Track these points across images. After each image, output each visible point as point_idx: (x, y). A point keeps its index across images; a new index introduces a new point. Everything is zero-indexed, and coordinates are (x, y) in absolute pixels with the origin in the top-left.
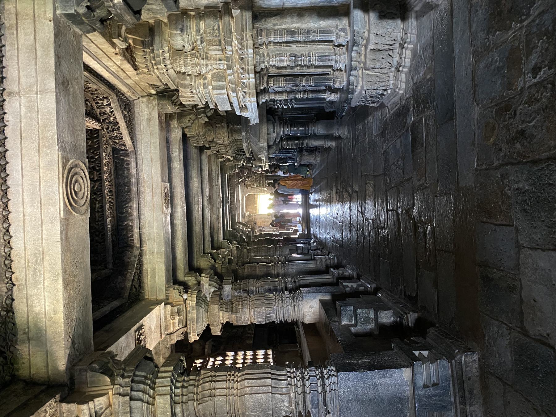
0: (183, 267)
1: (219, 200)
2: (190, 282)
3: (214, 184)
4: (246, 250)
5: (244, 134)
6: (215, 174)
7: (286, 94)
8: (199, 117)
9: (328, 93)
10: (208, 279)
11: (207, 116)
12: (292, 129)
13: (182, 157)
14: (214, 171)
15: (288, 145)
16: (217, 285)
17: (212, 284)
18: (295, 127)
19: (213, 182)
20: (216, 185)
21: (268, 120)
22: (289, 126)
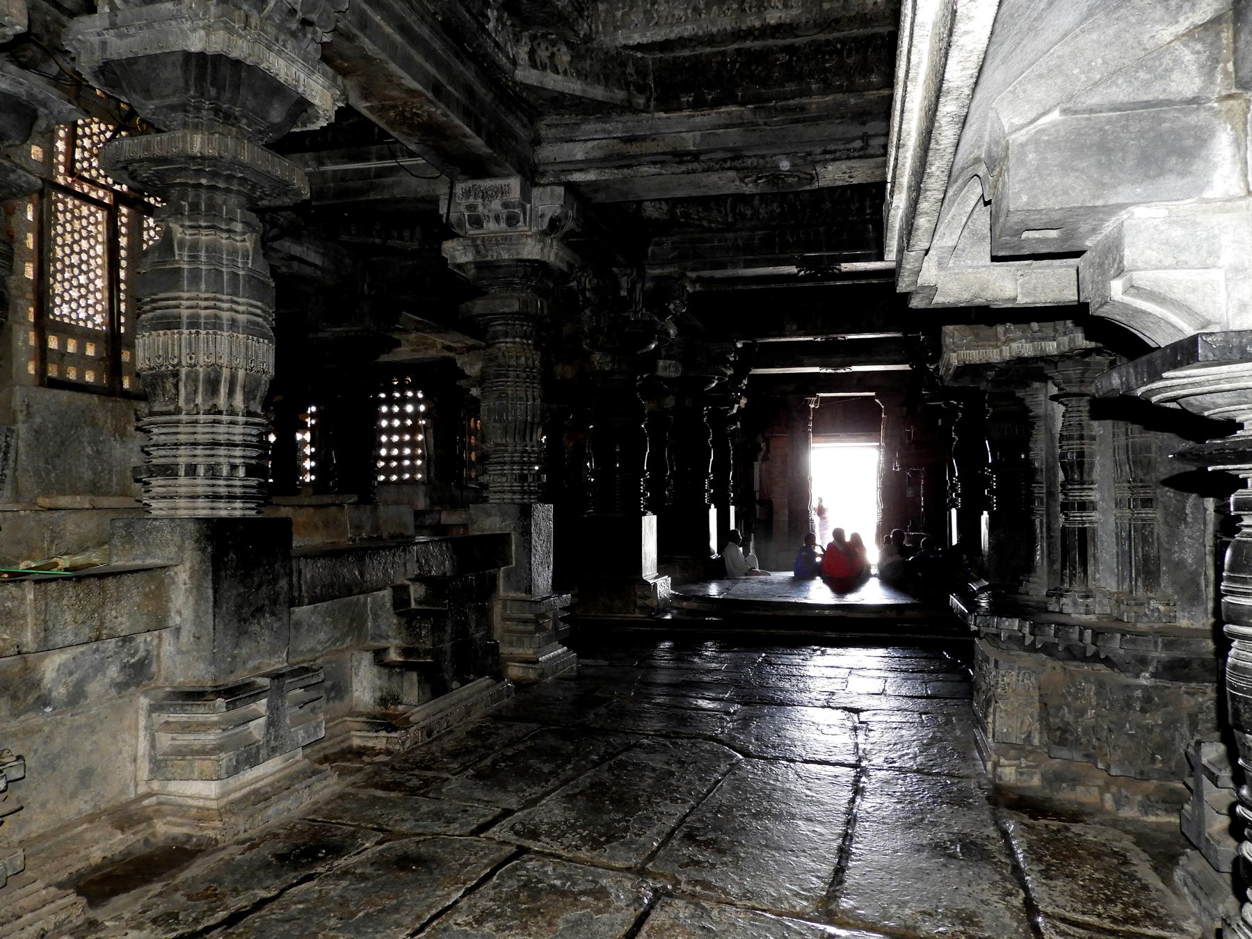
20: (866, 138)
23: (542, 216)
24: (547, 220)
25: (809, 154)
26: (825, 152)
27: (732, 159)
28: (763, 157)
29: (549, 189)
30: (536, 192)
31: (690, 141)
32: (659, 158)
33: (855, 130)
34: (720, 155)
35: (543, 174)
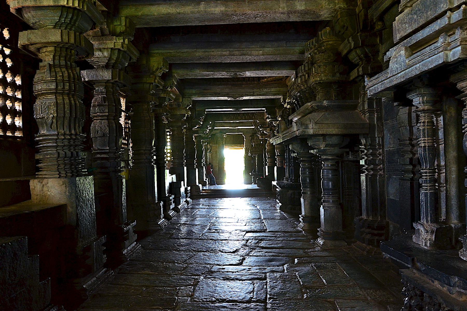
0: (140, 14)
1: (237, 95)
2: (119, 23)
3: (255, 90)
4: (180, 124)
5: (325, 103)
6: (267, 92)
7: (430, 144)
8: (350, 39)
9: (434, 227)
10: (119, 47)
11: (350, 51)
12: (330, 172)
13: (293, 18)
14: (270, 91)
15: (304, 169)
16: (113, 61)
17: (114, 54)
18: (332, 176)
19: (258, 89)
20: (253, 92)
21: (343, 136)
22: (334, 168)
23: (185, 104)
24: (186, 105)
25: (243, 95)
26: (246, 95)
27: (227, 95)
28: (233, 95)
29: (187, 98)
30: (184, 99)
31: (218, 91)
32: (211, 94)
33: (252, 91)
34: (225, 94)
35: (186, 95)
